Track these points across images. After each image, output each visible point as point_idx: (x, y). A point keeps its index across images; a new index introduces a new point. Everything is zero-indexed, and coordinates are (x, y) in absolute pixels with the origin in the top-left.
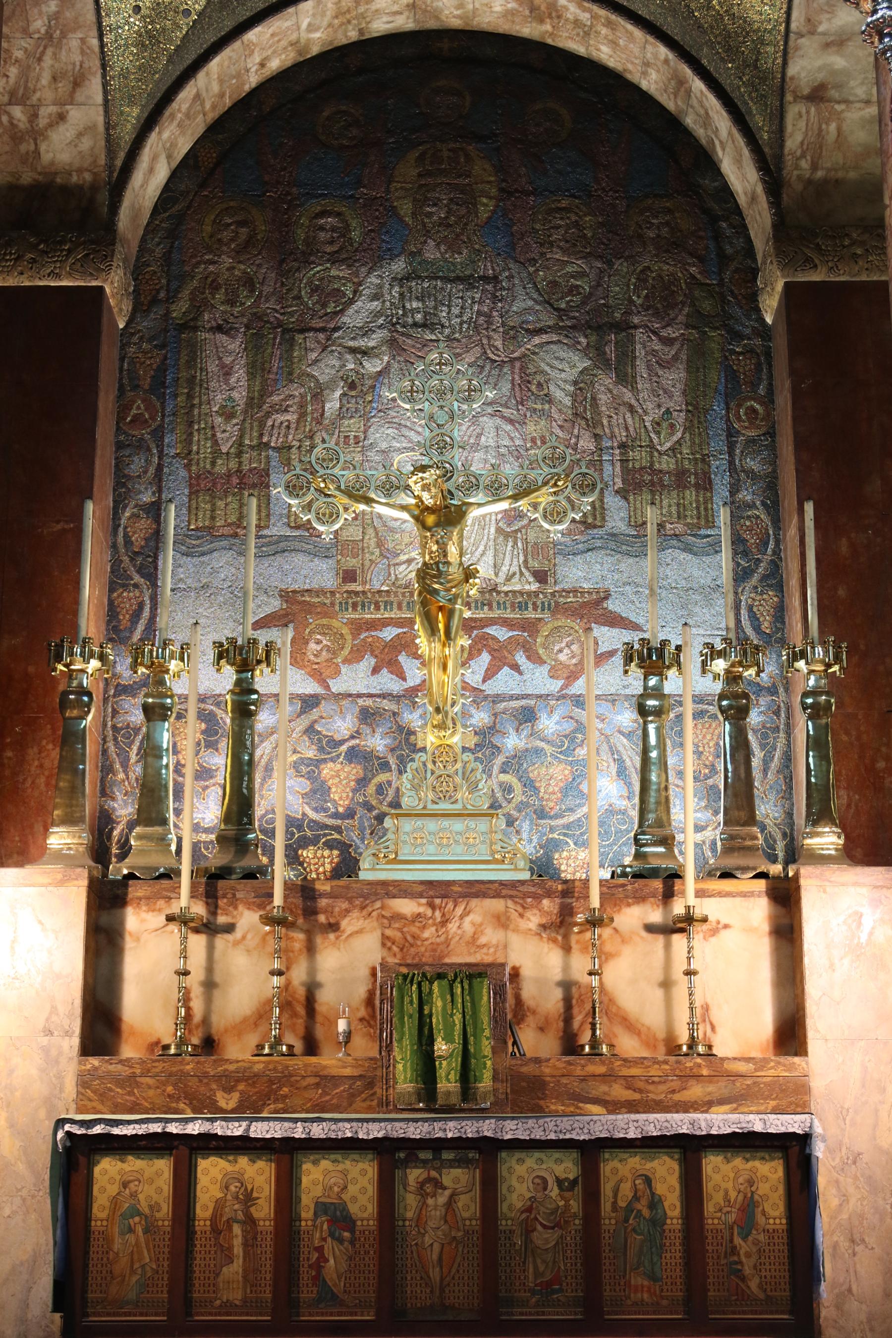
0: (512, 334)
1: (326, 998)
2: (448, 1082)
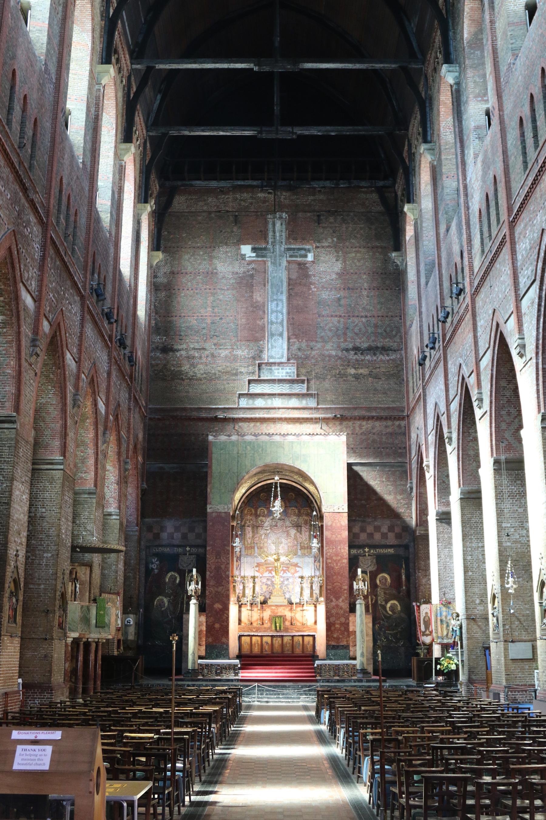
0: (286, 527)
1: (264, 618)
2: (278, 628)
